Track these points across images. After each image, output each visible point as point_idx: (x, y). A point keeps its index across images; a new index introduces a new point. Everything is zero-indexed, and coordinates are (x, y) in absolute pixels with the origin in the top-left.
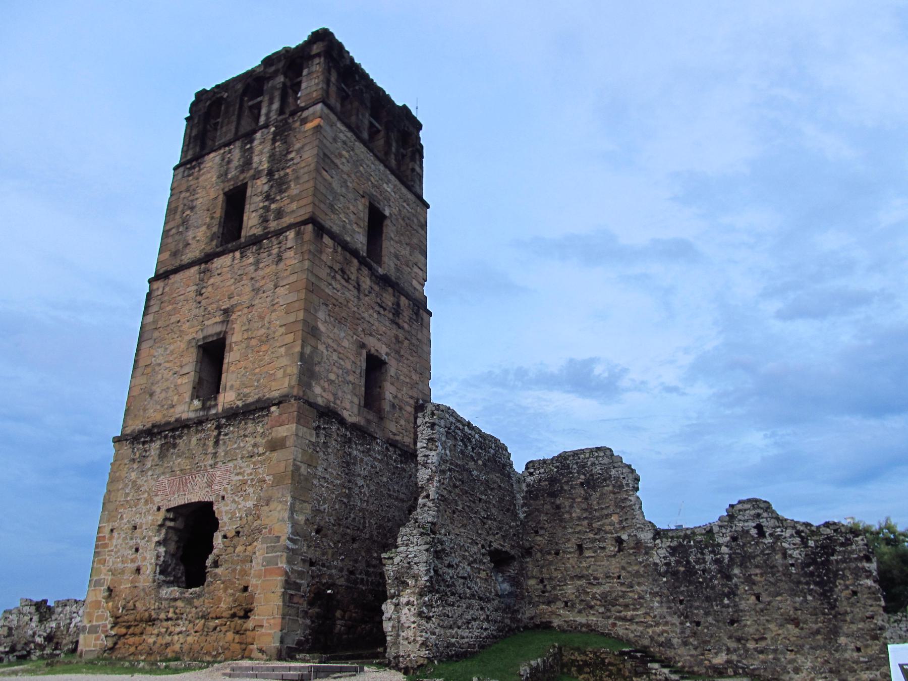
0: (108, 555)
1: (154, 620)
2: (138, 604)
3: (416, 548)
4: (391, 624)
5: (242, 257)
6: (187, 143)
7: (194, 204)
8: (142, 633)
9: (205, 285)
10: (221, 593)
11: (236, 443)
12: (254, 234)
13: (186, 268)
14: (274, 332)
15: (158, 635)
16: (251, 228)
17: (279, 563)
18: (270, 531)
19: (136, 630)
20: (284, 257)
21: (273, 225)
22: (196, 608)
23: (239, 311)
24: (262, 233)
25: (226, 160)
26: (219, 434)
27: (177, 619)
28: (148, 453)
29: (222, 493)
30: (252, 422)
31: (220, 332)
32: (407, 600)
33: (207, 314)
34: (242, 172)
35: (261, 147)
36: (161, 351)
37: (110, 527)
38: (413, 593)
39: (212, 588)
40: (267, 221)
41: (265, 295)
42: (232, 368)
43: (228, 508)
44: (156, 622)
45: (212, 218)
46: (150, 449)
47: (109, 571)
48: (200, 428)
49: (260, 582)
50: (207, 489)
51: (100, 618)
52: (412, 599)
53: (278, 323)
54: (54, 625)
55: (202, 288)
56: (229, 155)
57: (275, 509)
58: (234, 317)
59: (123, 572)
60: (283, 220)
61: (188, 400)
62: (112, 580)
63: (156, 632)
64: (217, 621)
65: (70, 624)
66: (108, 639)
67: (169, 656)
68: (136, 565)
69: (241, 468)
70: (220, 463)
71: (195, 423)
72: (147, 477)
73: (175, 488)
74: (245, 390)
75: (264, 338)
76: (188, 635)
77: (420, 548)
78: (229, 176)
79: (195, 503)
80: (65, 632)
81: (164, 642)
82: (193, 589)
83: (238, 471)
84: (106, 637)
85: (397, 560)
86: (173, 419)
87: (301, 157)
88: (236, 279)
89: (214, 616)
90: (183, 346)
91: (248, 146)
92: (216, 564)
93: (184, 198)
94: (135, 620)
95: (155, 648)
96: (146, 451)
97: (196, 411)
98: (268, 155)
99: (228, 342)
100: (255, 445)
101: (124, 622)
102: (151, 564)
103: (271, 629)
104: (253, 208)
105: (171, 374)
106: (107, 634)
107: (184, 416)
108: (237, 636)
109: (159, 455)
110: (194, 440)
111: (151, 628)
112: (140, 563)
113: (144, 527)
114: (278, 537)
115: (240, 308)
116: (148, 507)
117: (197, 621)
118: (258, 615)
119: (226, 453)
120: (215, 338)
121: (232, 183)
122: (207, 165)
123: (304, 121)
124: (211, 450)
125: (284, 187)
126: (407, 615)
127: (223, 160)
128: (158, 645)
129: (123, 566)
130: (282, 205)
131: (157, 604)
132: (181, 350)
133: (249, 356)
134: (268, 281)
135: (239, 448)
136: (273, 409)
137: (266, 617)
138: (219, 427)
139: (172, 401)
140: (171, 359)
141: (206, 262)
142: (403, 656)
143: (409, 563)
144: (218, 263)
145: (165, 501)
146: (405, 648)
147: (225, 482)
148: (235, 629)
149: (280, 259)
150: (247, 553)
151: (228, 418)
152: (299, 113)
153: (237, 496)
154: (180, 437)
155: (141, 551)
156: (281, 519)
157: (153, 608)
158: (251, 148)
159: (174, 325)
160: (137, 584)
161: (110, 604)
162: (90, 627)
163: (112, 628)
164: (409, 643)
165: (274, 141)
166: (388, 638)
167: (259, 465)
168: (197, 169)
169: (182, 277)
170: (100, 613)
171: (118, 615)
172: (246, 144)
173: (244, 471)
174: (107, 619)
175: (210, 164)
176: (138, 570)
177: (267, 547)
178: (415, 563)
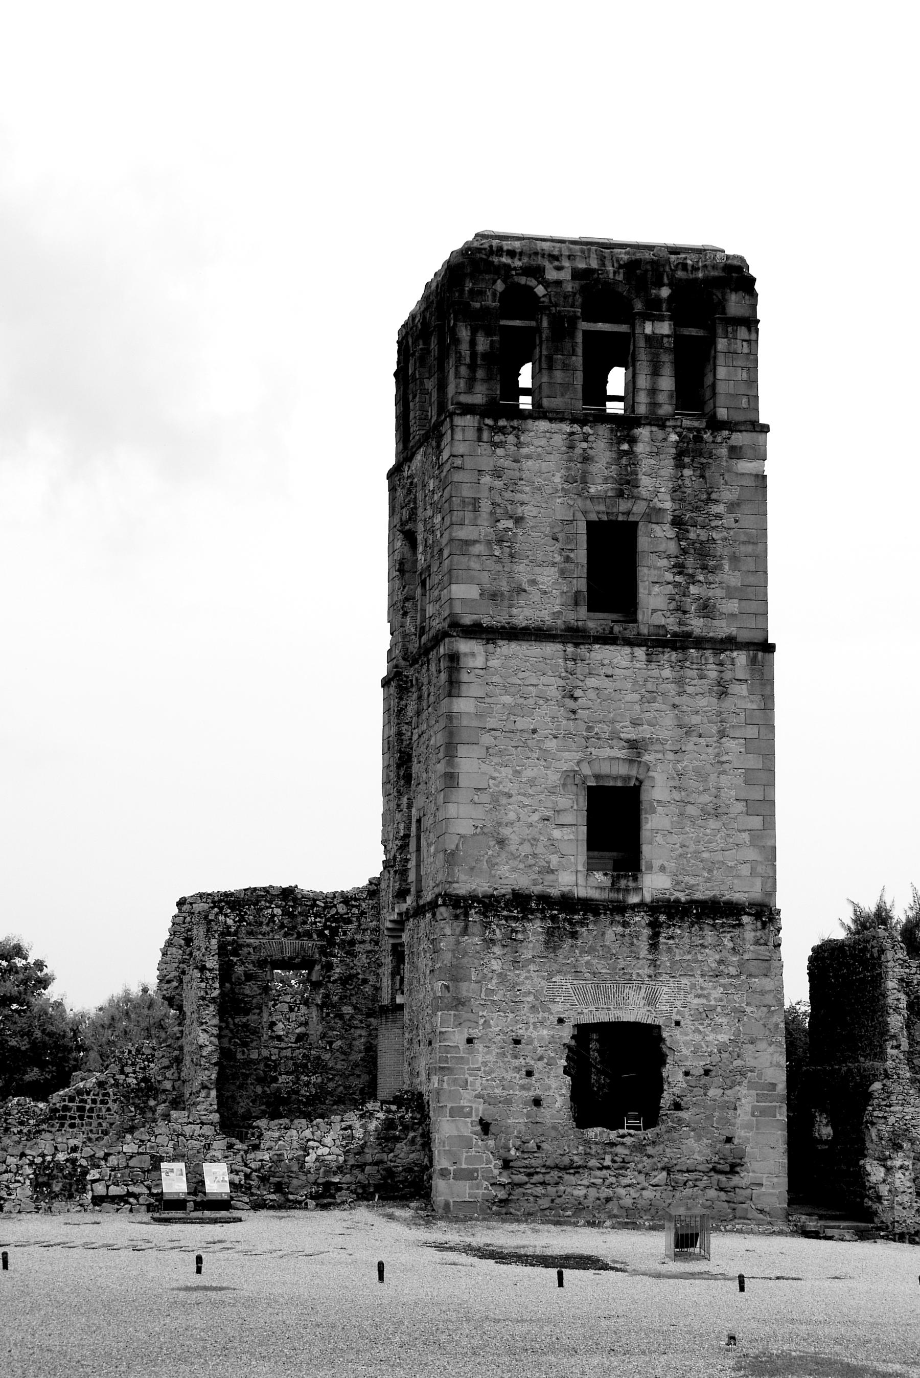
0: (471, 1075)
1: (579, 1167)
2: (545, 1146)
3: (913, 1109)
4: (887, 1188)
5: (649, 661)
6: (468, 361)
7: (519, 511)
8: (557, 1184)
9: (580, 684)
10: (691, 1142)
11: (689, 953)
12: (663, 626)
13: (535, 641)
14: (728, 806)
15: (588, 1187)
16: (654, 611)
17: (778, 1115)
18: (760, 1075)
19: (547, 1177)
20: (730, 691)
21: (697, 625)
22: (649, 1156)
23: (656, 751)
24: (676, 629)
25: (578, 451)
26: (655, 936)
27: (621, 1168)
28: (520, 936)
29: (675, 1017)
30: (711, 928)
31: (629, 778)
32: (901, 1163)
33: (591, 737)
34: (620, 494)
35: (653, 462)
36: (506, 772)
37: (466, 1036)
38: (908, 1157)
39: (675, 1135)
40: (685, 612)
41: (702, 740)
42: (659, 839)
43: (687, 1038)
44: (581, 1170)
45: (568, 559)
46: (524, 931)
47: (479, 1096)
48: (618, 918)
49: (751, 1134)
50: (649, 1008)
51: (469, 1160)
52: (906, 1163)
53: (733, 793)
54: (267, 1157)
55: (576, 687)
56: (585, 445)
57: (765, 1050)
58: (646, 758)
59: (508, 1101)
60: (716, 623)
61: (580, 868)
62: (484, 1110)
63: (585, 1182)
64: (686, 1175)
65: (305, 1156)
66: (494, 1187)
67: (615, 1211)
68: (532, 1093)
69: (702, 988)
70: (665, 977)
71: (609, 909)
72: (529, 971)
73: (589, 997)
74: (687, 878)
75: (710, 808)
76: (643, 1189)
77: (917, 1110)
78: (592, 490)
79: (628, 1023)
80: (295, 1168)
81: (603, 1196)
82: (621, 1131)
83: (700, 992)
84: (492, 1185)
85: (892, 1120)
86: (555, 892)
87: (736, 521)
88: (643, 697)
89: (685, 1169)
90: (554, 778)
91: (625, 447)
92: (677, 1107)
93: (491, 489)
94: (544, 1166)
95: (589, 1202)
96: (517, 932)
97: (602, 889)
98: (670, 485)
99: (644, 797)
100: (721, 962)
101: (524, 1167)
102: (561, 1095)
103: (773, 1188)
104: (653, 575)
105: (536, 817)
106: (495, 1181)
107: (581, 892)
108: (722, 1193)
109: (546, 943)
110: (610, 934)
111: (572, 1177)
112: (538, 1092)
113: (536, 1043)
114: (774, 1086)
115: (658, 747)
116: (540, 1015)
117: (656, 1173)
118: (754, 1172)
119: (673, 963)
120: (619, 784)
121: (602, 508)
122: (536, 442)
123: (735, 452)
124: (644, 953)
125: (711, 563)
126: (902, 1180)
127: (571, 447)
128: (591, 1199)
129: (505, 1093)
130: (711, 594)
131: (581, 1148)
132: (549, 782)
133: (688, 829)
134: (706, 721)
135: (697, 961)
136: (745, 919)
137: (766, 1175)
138: (654, 925)
139: (548, 862)
140: (530, 792)
141: (576, 645)
142: (898, 1222)
143: (905, 1124)
144: (601, 653)
145: (572, 1013)
146: (899, 1213)
147: (678, 1003)
148: (718, 1185)
149: (722, 690)
150: (726, 1098)
151: (670, 917)
152: (727, 432)
153: (702, 1024)
154: (582, 923)
155: (536, 1075)
156: (774, 1063)
157: (575, 1152)
158: (630, 453)
159: (526, 735)
160: (538, 1120)
161: (491, 1143)
162: (454, 1170)
163: (500, 1173)
164: (904, 1208)
165: (679, 465)
166: (885, 1203)
167: (733, 991)
168: (511, 439)
169: (528, 653)
170: (474, 1153)
171: (510, 1158)
172: (620, 442)
173: (709, 994)
174: (488, 1162)
175: (543, 442)
176: (537, 1102)
177: (757, 1094)
178: (912, 1126)
